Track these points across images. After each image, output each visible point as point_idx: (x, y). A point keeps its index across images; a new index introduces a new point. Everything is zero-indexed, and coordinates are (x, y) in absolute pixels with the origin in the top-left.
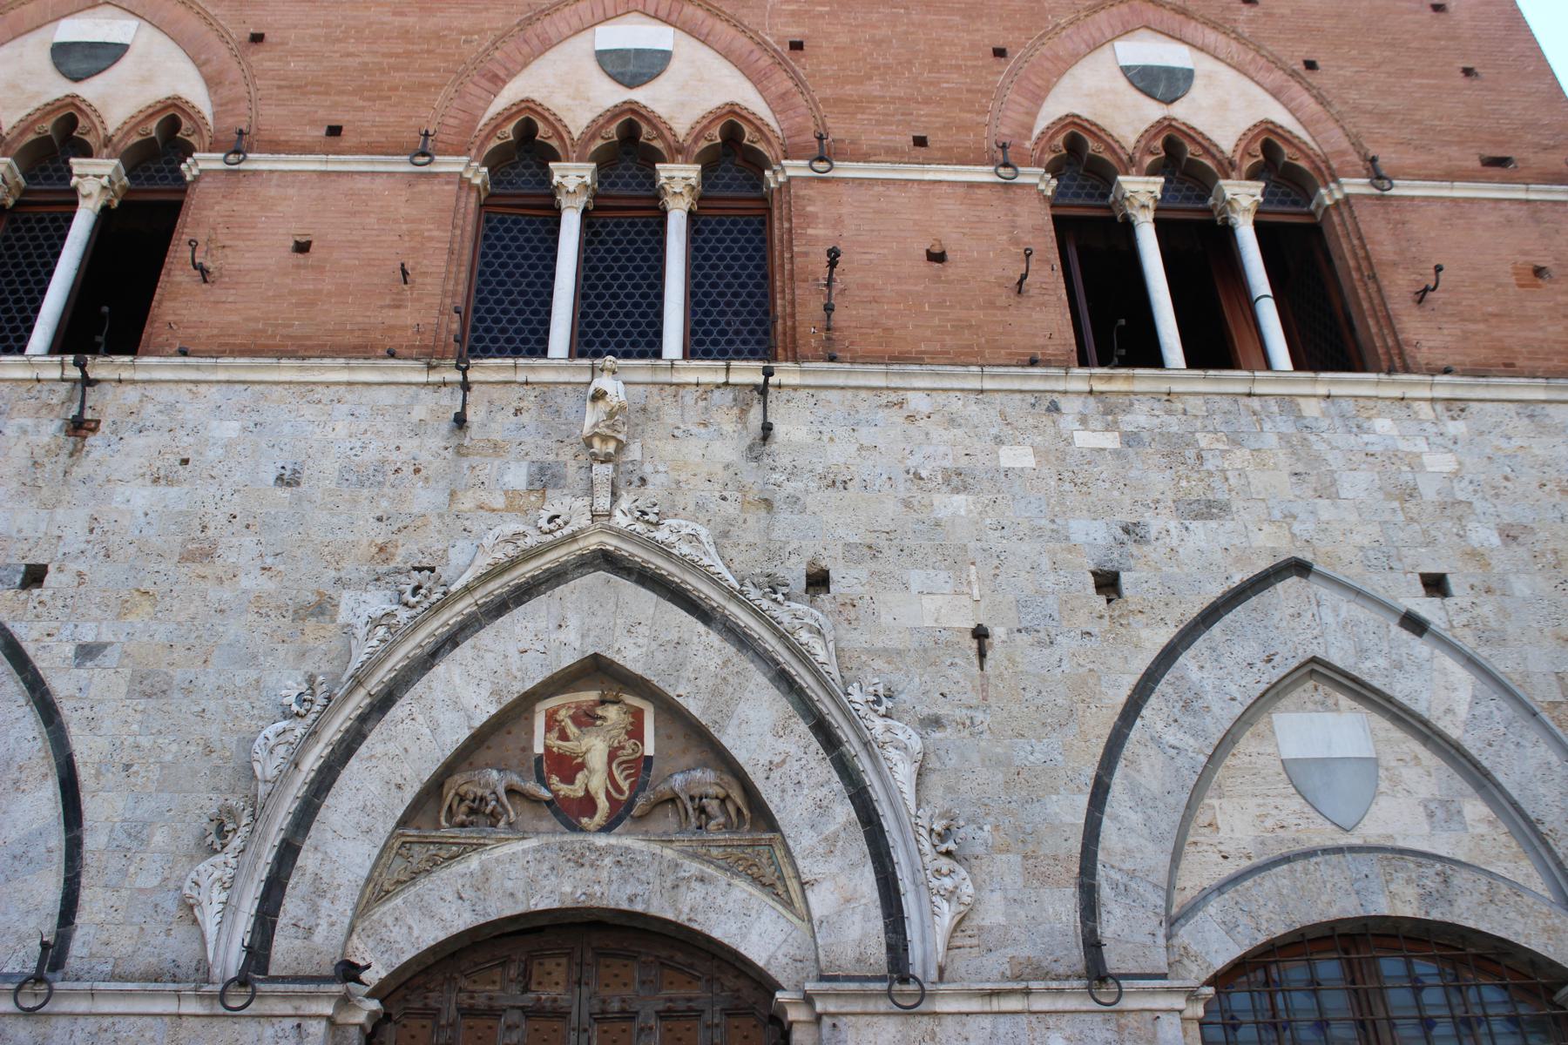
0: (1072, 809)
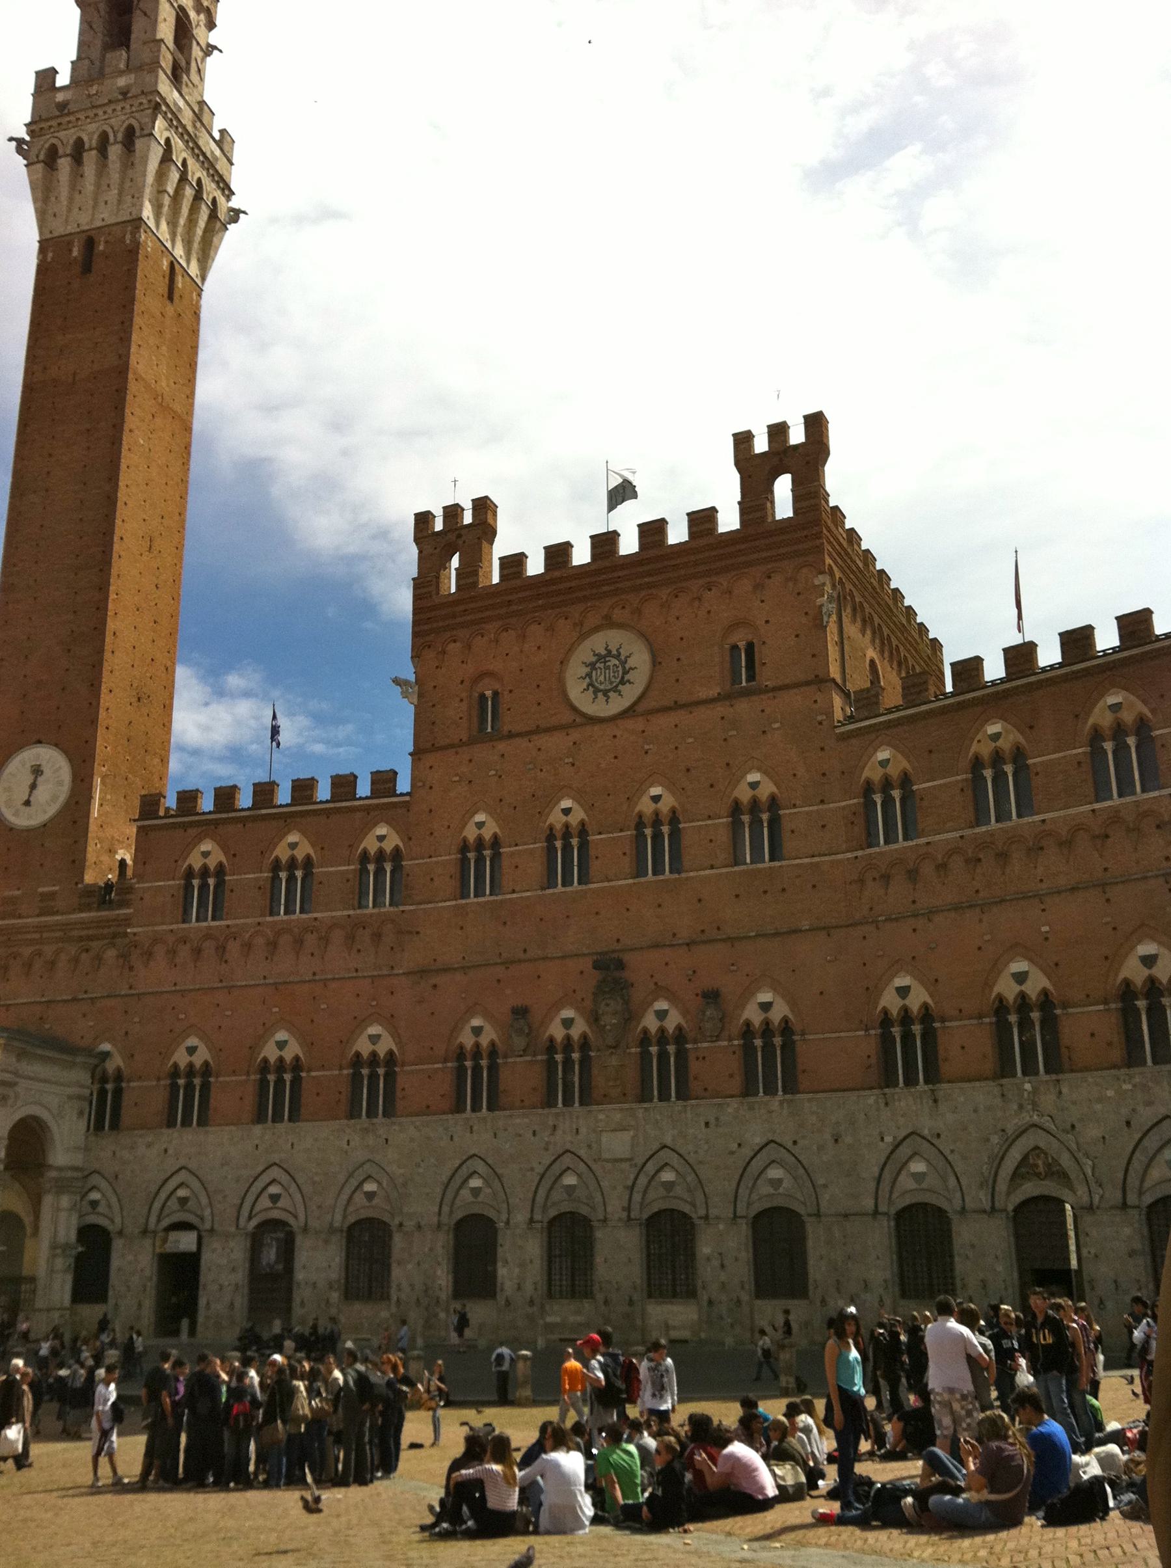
0: (1121, 1175)
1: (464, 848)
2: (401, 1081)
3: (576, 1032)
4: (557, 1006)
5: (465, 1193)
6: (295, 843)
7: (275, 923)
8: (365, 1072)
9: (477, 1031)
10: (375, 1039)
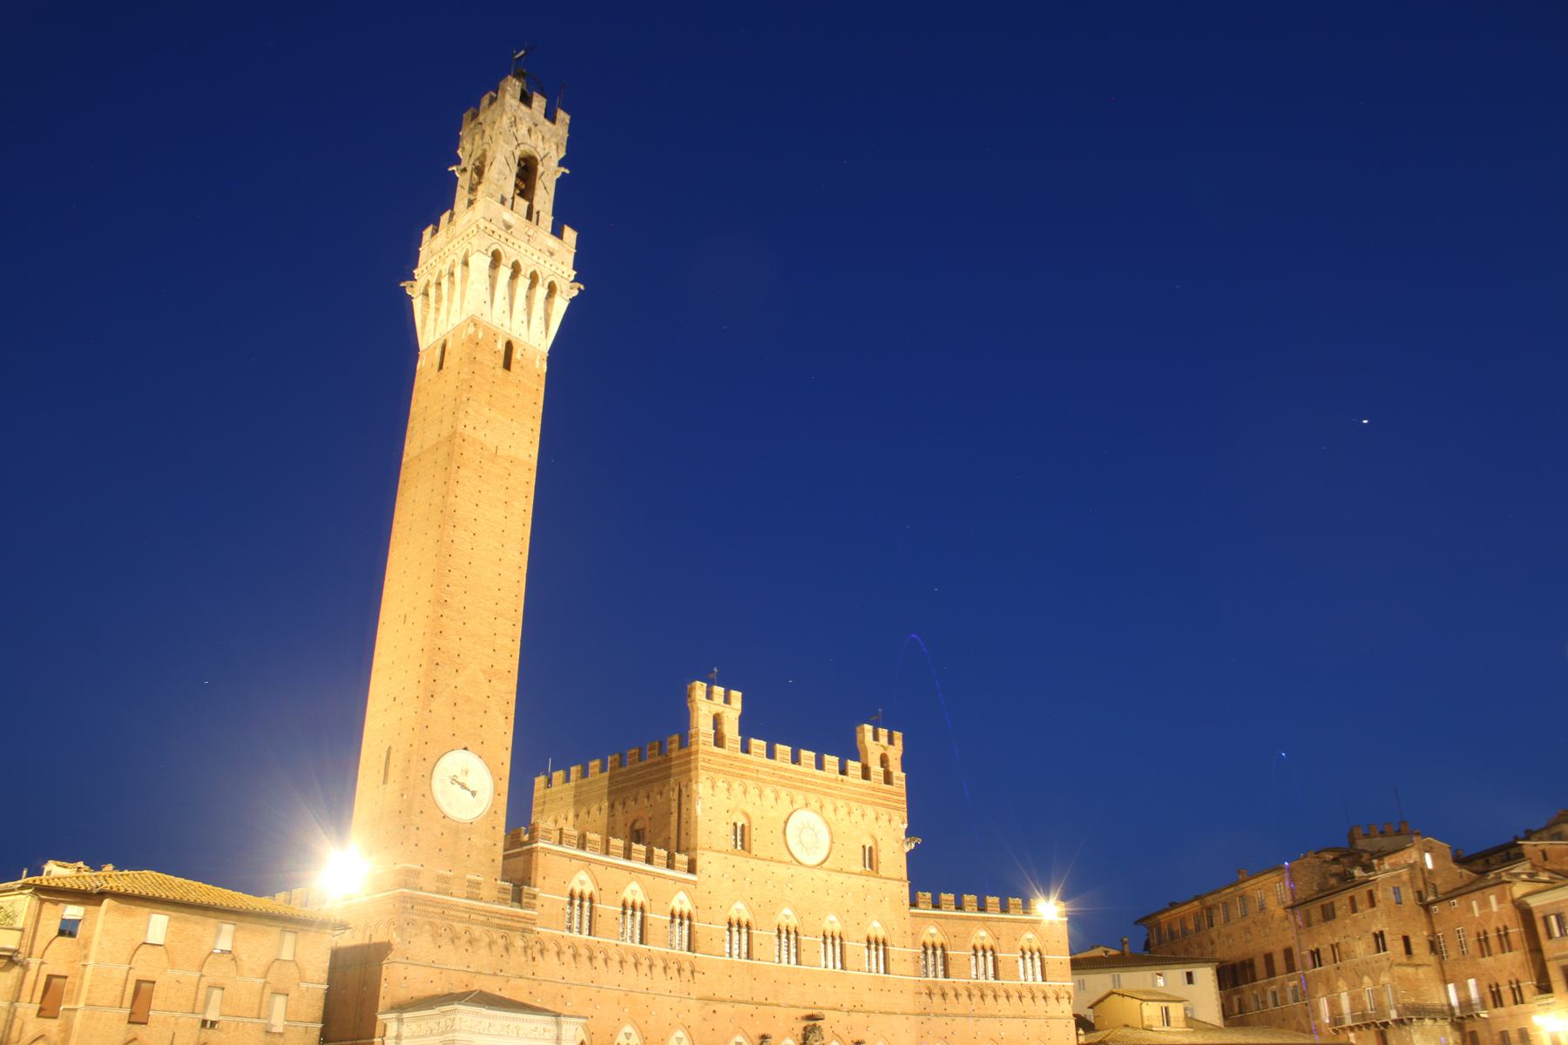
7: (626, 948)
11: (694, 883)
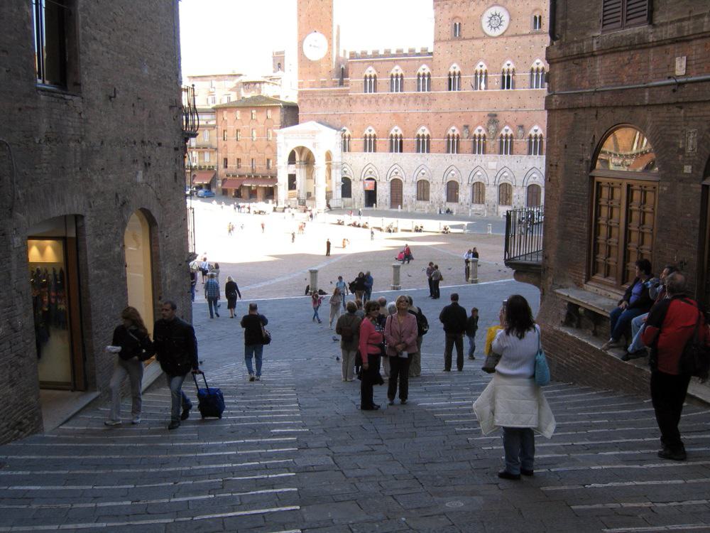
1: (450, 75)
2: (431, 143)
3: (482, 134)
4: (477, 125)
5: (450, 175)
6: (397, 70)
8: (421, 140)
9: (454, 131)
10: (423, 131)
11: (432, 59)
